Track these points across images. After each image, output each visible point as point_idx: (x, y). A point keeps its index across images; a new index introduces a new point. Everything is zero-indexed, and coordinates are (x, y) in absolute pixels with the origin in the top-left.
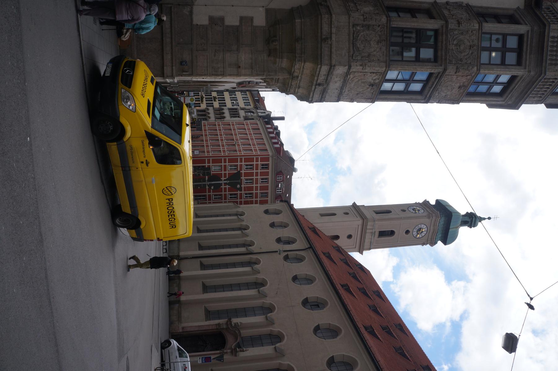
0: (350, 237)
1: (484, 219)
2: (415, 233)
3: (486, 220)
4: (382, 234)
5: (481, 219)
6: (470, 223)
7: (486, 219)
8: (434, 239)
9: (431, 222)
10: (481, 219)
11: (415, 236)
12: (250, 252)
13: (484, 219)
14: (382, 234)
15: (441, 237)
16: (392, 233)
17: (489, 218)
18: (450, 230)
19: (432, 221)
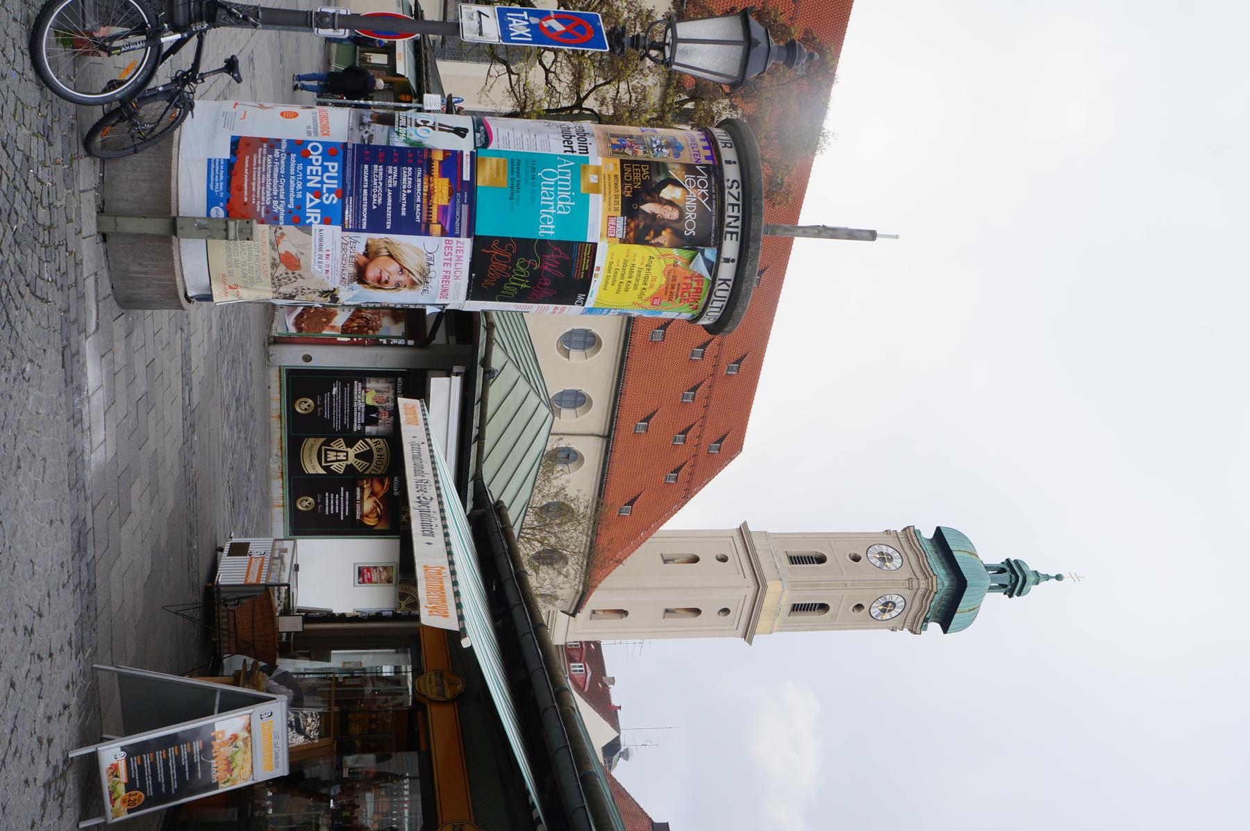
1: (1047, 577)
3: (1050, 580)
5: (1039, 579)
6: (1008, 569)
7: (1052, 577)
8: (926, 569)
9: (899, 540)
10: (1039, 579)
11: (878, 564)
12: (488, 416)
13: (1047, 577)
15: (947, 574)
16: (821, 560)
17: (1058, 577)
18: (955, 554)
19: (900, 539)
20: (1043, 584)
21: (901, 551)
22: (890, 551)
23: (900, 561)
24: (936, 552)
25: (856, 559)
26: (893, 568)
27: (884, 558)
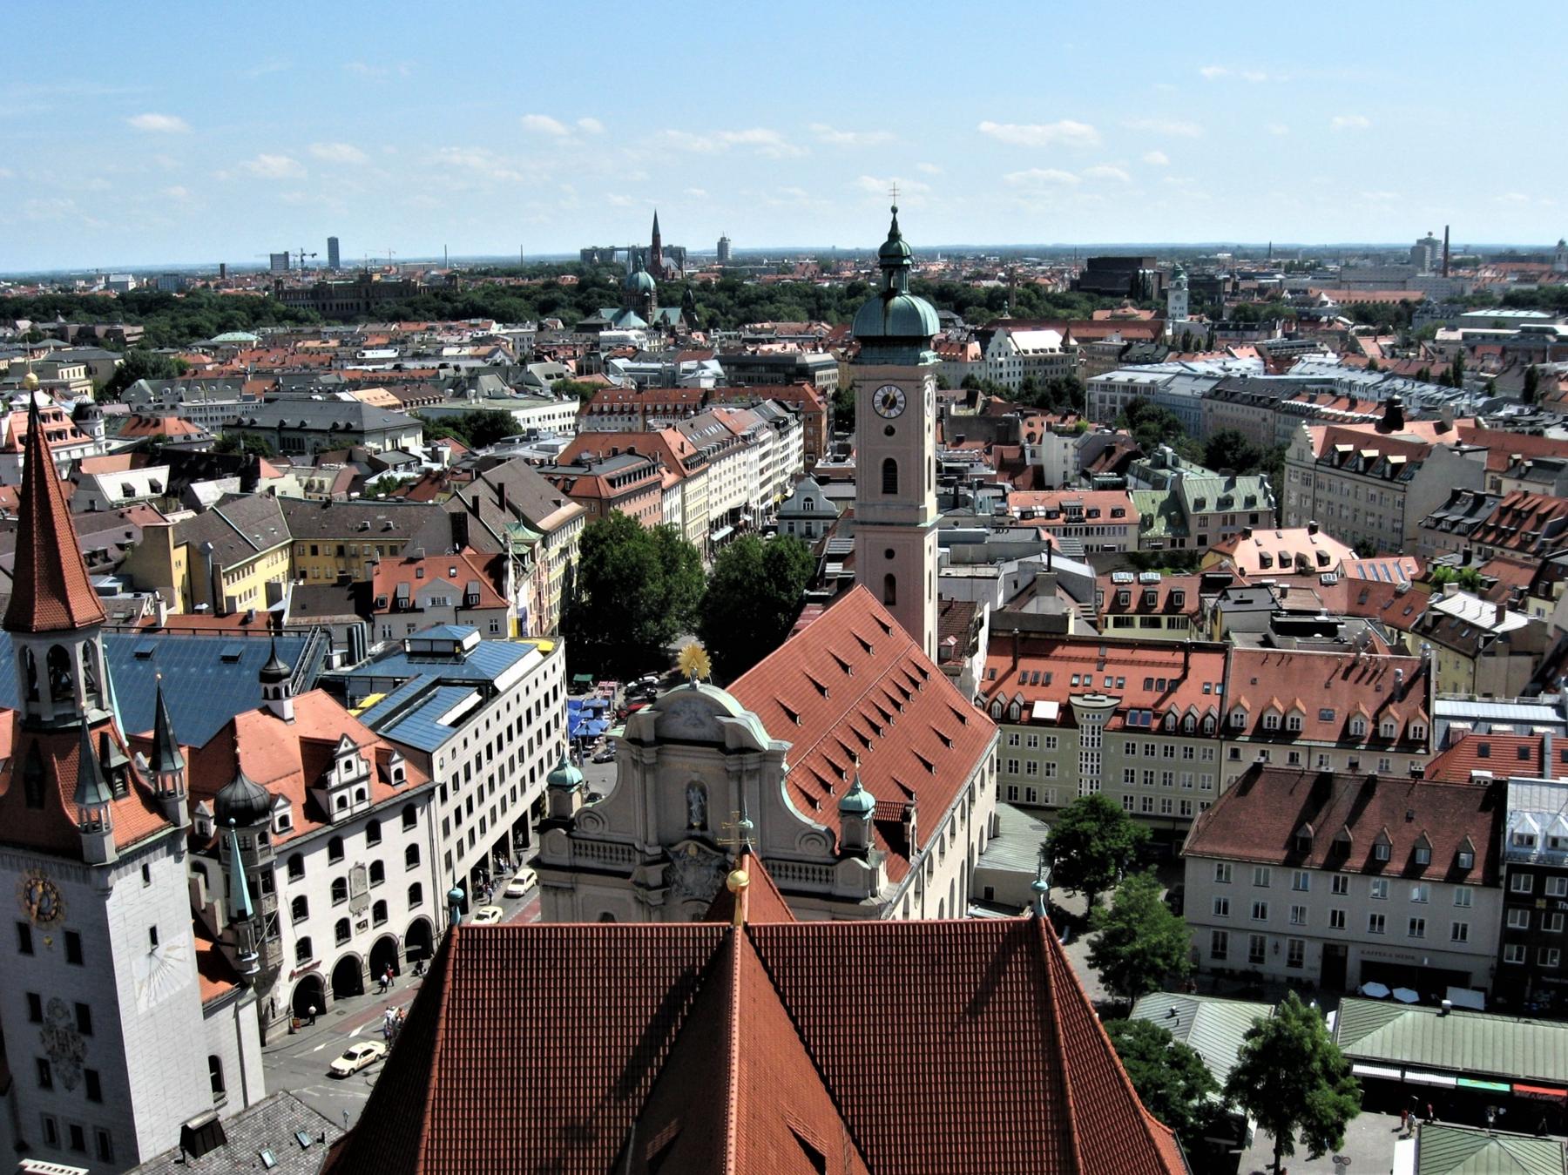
0: (890, 554)
1: (894, 224)
2: (894, 413)
4: (890, 486)
5: (894, 235)
7: (894, 219)
10: (894, 235)
13: (894, 224)
14: (890, 486)
16: (890, 467)
17: (894, 210)
18: (889, 333)
20: (901, 228)
21: (881, 384)
22: (880, 392)
23: (894, 389)
24: (881, 346)
25: (890, 431)
26: (902, 398)
27: (889, 402)
